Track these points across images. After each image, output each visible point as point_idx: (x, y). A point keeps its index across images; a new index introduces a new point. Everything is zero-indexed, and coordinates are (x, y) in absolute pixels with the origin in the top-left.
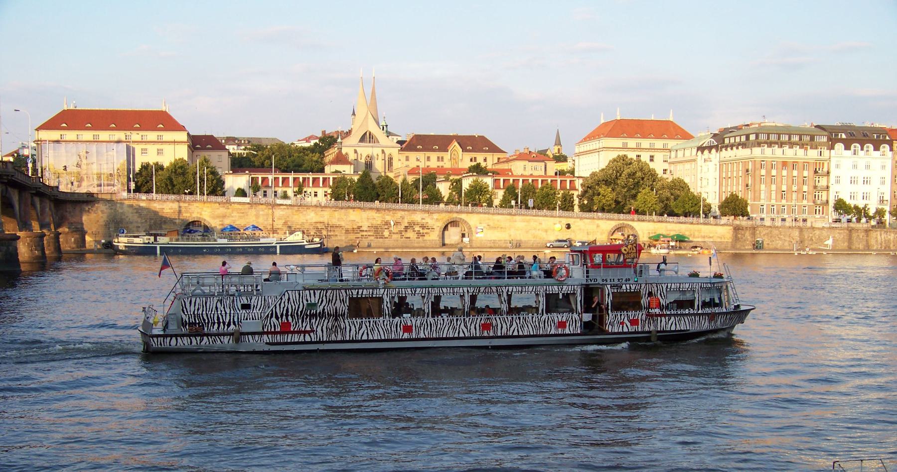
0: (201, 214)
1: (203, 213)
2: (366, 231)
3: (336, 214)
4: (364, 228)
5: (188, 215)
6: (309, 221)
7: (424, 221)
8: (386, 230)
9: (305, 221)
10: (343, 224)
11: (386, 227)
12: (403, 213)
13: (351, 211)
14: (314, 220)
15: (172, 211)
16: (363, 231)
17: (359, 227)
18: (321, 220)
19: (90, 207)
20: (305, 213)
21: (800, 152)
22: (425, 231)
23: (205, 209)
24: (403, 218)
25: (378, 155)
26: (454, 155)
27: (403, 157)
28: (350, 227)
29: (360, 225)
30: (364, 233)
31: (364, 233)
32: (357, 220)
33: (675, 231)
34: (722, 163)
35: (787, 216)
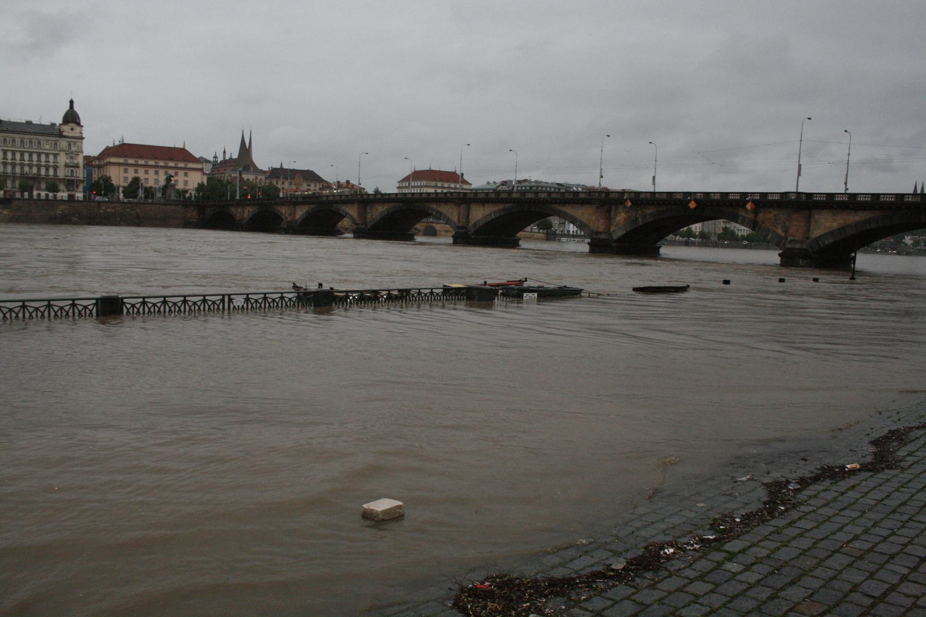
22: (416, 232)
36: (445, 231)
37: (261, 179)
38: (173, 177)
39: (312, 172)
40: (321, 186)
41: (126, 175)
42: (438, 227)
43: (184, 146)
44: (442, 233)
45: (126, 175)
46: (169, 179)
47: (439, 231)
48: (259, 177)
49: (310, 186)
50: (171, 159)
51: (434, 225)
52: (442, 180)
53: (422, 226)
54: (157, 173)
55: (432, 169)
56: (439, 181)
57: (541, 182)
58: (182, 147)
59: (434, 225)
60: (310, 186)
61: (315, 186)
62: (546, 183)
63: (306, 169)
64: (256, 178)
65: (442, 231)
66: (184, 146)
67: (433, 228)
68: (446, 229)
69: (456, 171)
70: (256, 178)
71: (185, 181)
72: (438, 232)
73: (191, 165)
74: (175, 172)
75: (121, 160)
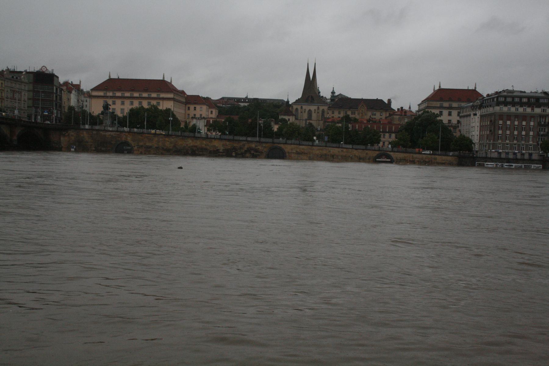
0: (127, 139)
1: (128, 138)
2: (221, 152)
3: (204, 142)
4: (221, 151)
5: (119, 139)
6: (189, 145)
7: (257, 148)
8: (234, 153)
9: (185, 145)
10: (208, 147)
11: (234, 150)
12: (244, 142)
13: (213, 140)
14: (191, 145)
15: (110, 136)
16: (220, 152)
17: (218, 150)
18: (196, 144)
19: (66, 132)
20: (186, 140)
21: (529, 110)
22: (257, 154)
23: (129, 136)
24: (244, 145)
25: (315, 110)
26: (362, 111)
27: (330, 112)
28: (212, 149)
29: (218, 148)
30: (221, 154)
31: (221, 154)
32: (217, 145)
33: (419, 158)
34: (482, 116)
35: (517, 152)
36: (297, 153)
37: (323, 110)
38: (110, 105)
39: (381, 100)
40: (388, 115)
41: (122, 107)
42: (287, 148)
43: (164, 78)
44: (293, 155)
45: (122, 107)
46: (106, 107)
47: (289, 153)
48: (321, 108)
49: (375, 115)
50: (146, 91)
51: (282, 146)
52: (450, 100)
53: (265, 147)
54: (123, 103)
55: (469, 89)
56: (446, 101)
57: (513, 92)
58: (162, 79)
59: (282, 146)
60: (375, 115)
61: (381, 115)
62: (521, 92)
63: (376, 98)
64: (318, 108)
65: (294, 153)
66: (164, 78)
67: (281, 149)
68: (298, 150)
69: (475, 88)
70: (318, 108)
71: (121, 109)
72: (287, 154)
73: (162, 95)
74: (113, 101)
75: (101, 94)
